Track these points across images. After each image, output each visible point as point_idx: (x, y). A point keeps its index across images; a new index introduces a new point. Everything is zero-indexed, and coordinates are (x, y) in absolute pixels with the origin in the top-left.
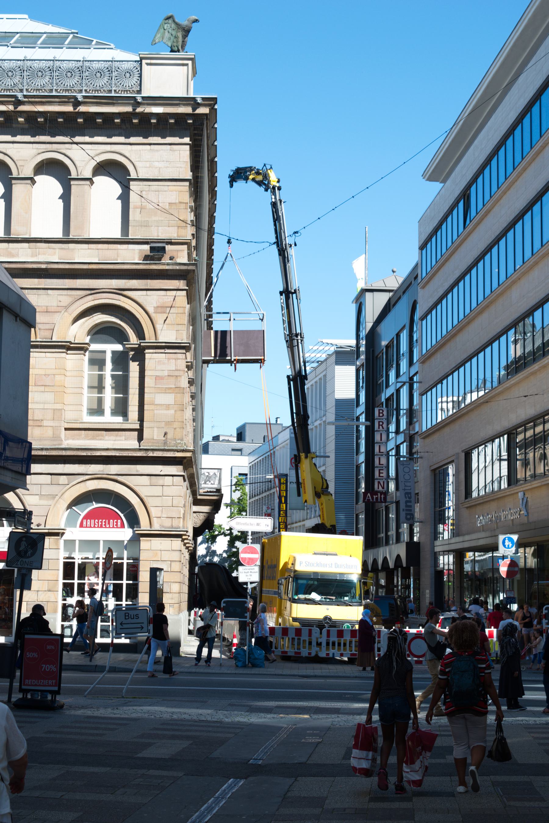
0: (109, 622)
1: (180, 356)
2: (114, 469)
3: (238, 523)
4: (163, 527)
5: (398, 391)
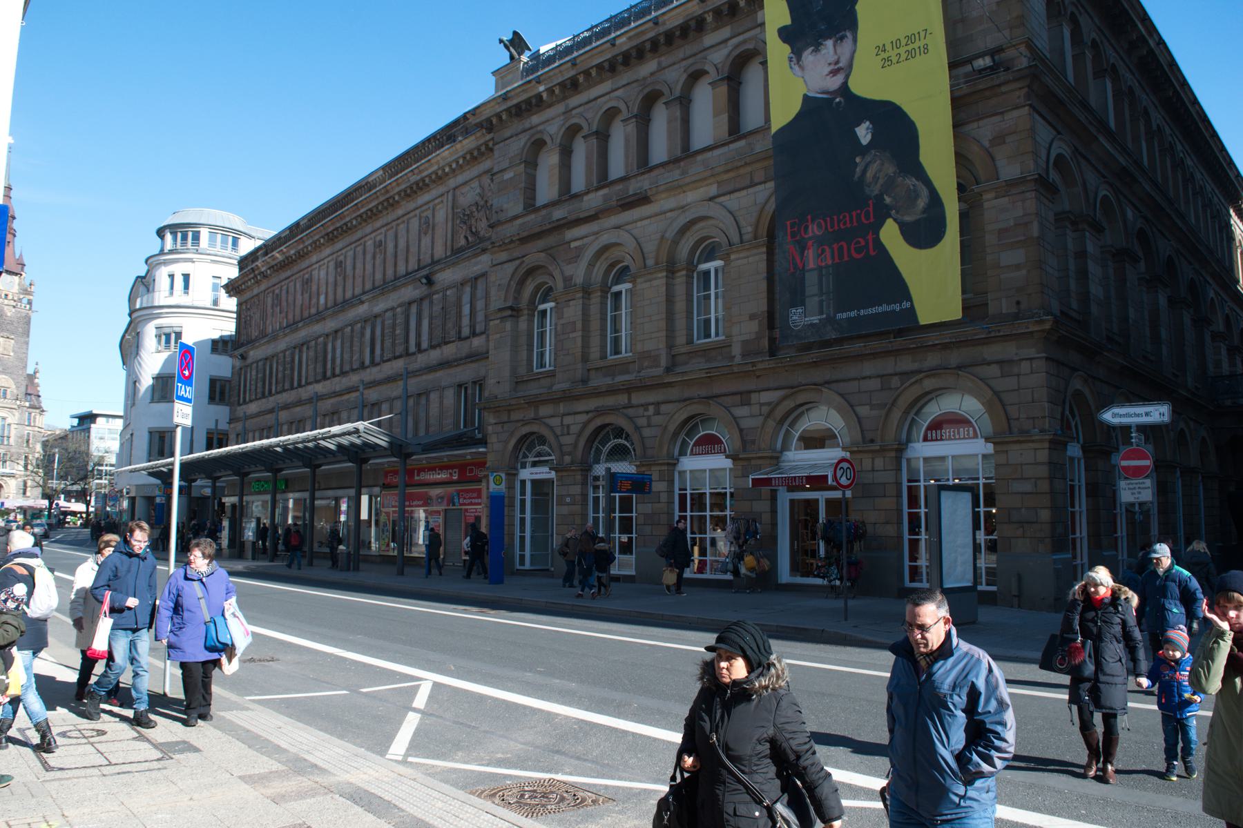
1: (1028, 195)
2: (954, 358)
3: (1114, 415)
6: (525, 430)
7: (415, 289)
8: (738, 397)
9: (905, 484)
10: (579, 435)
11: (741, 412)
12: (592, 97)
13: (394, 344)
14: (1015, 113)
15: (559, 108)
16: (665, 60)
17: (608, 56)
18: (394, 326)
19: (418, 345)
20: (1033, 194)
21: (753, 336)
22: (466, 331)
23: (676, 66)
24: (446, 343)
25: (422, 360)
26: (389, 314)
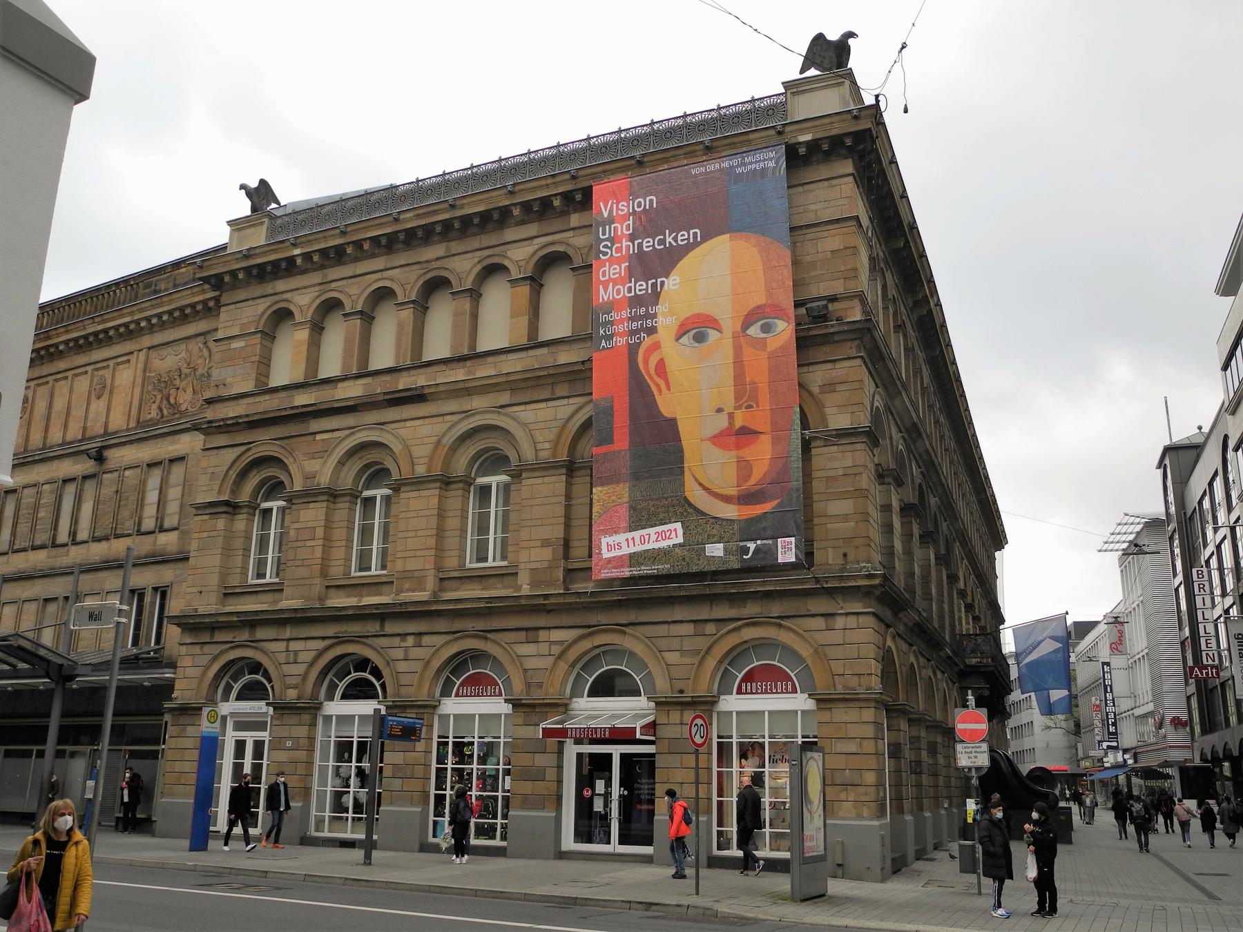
0: (622, 841)
1: (858, 446)
2: (776, 609)
4: (848, 688)
5: (1219, 547)
6: (233, 655)
7: (76, 463)
8: (522, 636)
9: (715, 740)
10: (311, 665)
11: (529, 649)
12: (358, 272)
13: (33, 530)
14: (847, 364)
15: (316, 277)
16: (456, 246)
17: (388, 230)
18: (36, 508)
19: (73, 534)
20: (863, 446)
21: (546, 565)
22: (149, 524)
23: (469, 255)
24: (117, 537)
25: (76, 555)
26: (32, 491)
